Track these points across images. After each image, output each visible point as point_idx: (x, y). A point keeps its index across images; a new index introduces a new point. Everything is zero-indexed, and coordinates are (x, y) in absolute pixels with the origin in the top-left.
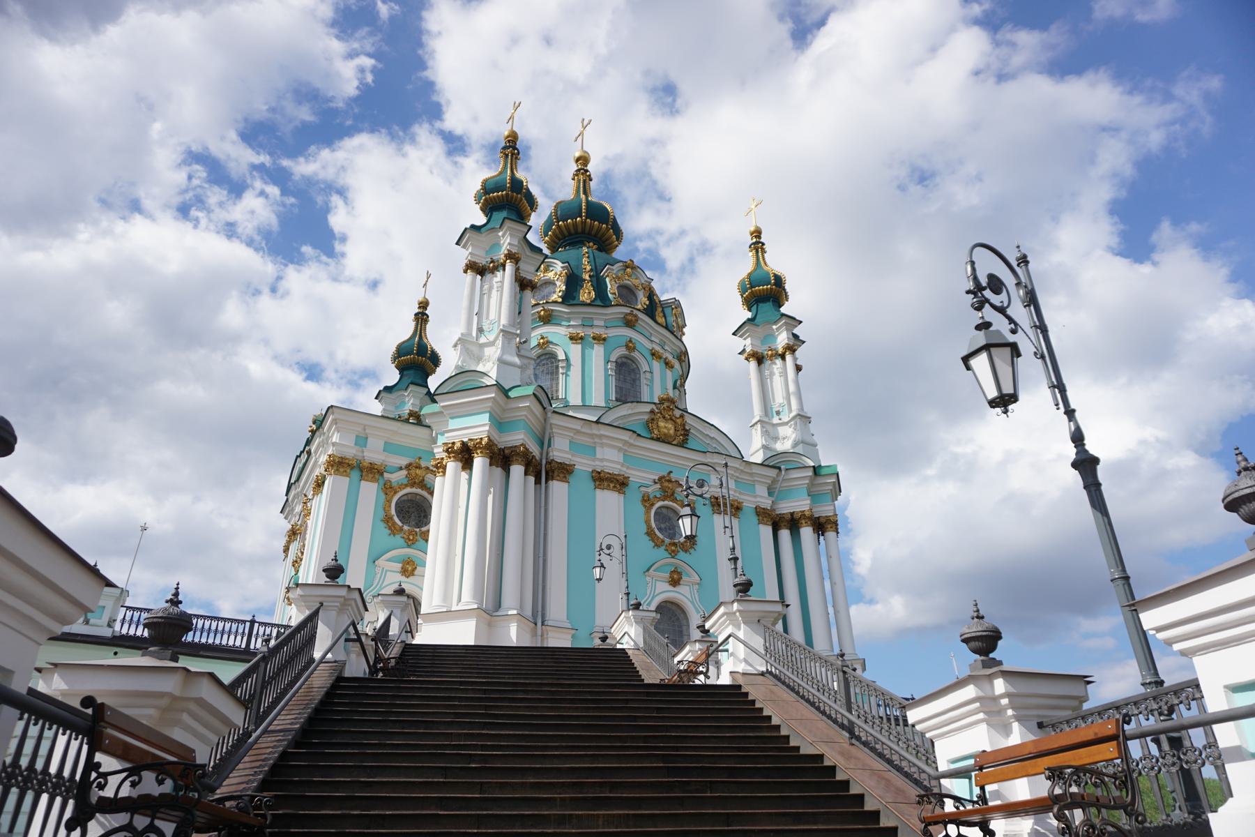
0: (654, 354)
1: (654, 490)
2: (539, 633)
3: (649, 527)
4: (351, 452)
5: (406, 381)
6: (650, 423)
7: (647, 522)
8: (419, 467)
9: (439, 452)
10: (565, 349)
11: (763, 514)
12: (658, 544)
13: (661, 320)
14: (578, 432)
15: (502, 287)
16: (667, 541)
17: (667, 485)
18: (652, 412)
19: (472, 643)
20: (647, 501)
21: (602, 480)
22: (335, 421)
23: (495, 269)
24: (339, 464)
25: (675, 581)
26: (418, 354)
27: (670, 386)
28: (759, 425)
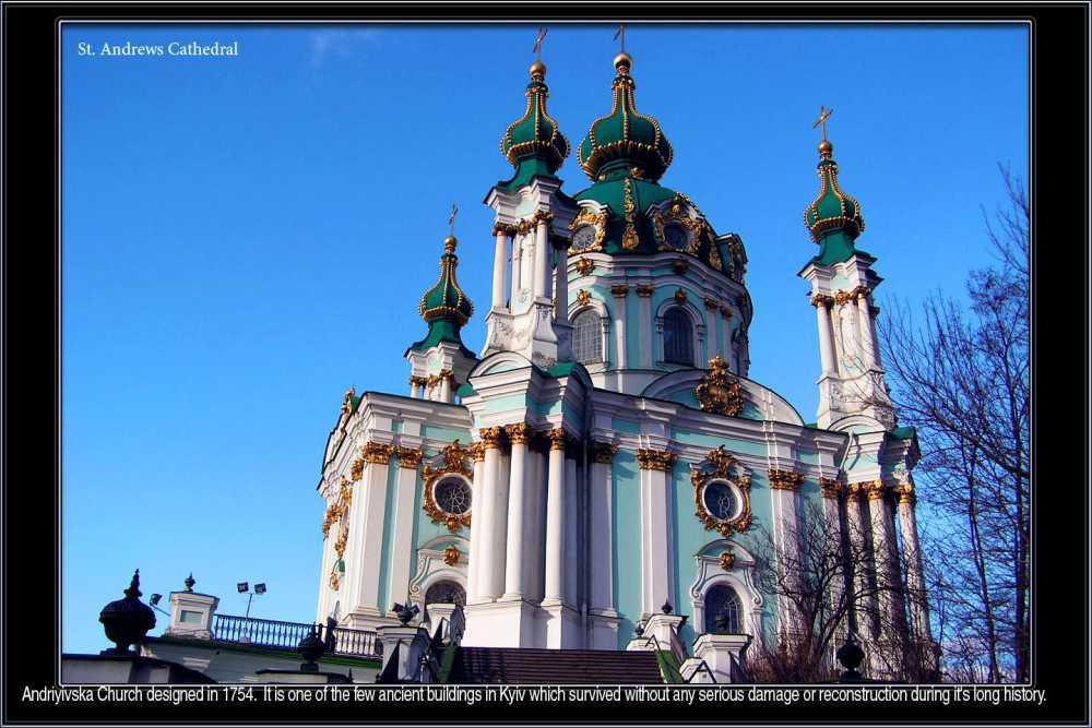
2: (585, 621)
3: (701, 507)
7: (698, 501)
8: (457, 450)
9: (476, 437)
11: (827, 485)
12: (711, 525)
13: (715, 261)
14: (619, 408)
15: (534, 251)
16: (720, 521)
19: (517, 646)
20: (700, 479)
21: (648, 458)
26: (447, 305)
27: (726, 338)
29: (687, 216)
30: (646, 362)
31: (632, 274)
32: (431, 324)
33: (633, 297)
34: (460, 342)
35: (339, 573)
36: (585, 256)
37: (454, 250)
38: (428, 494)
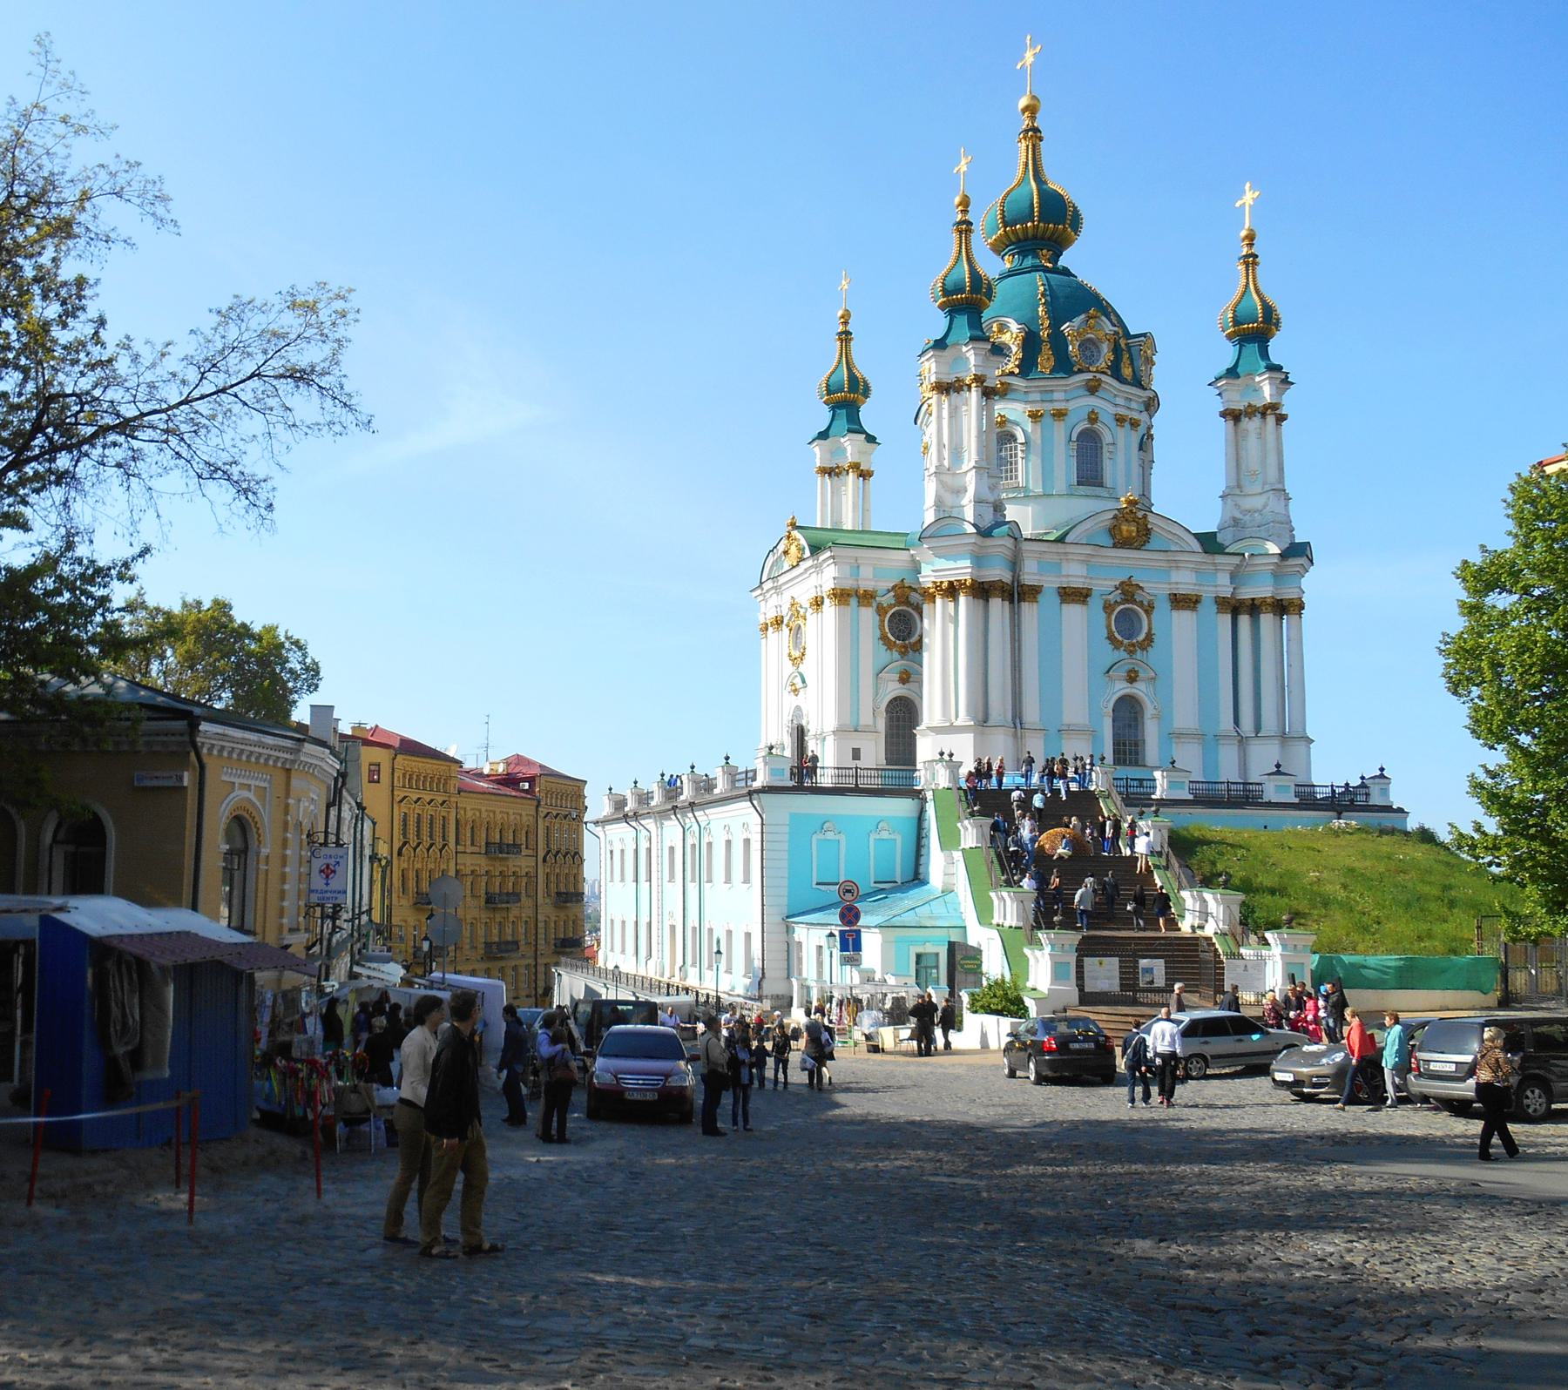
0: (1120, 420)
1: (1116, 596)
4: (848, 584)
5: (842, 423)
6: (1113, 531)
11: (1223, 604)
17: (1128, 590)
18: (1115, 517)
20: (1108, 608)
22: (833, 557)
23: (959, 390)
25: (1132, 678)
28: (1229, 500)
30: (1060, 486)
31: (1048, 397)
32: (833, 409)
33: (1048, 420)
34: (862, 431)
35: (799, 684)
36: (1004, 379)
38: (881, 627)
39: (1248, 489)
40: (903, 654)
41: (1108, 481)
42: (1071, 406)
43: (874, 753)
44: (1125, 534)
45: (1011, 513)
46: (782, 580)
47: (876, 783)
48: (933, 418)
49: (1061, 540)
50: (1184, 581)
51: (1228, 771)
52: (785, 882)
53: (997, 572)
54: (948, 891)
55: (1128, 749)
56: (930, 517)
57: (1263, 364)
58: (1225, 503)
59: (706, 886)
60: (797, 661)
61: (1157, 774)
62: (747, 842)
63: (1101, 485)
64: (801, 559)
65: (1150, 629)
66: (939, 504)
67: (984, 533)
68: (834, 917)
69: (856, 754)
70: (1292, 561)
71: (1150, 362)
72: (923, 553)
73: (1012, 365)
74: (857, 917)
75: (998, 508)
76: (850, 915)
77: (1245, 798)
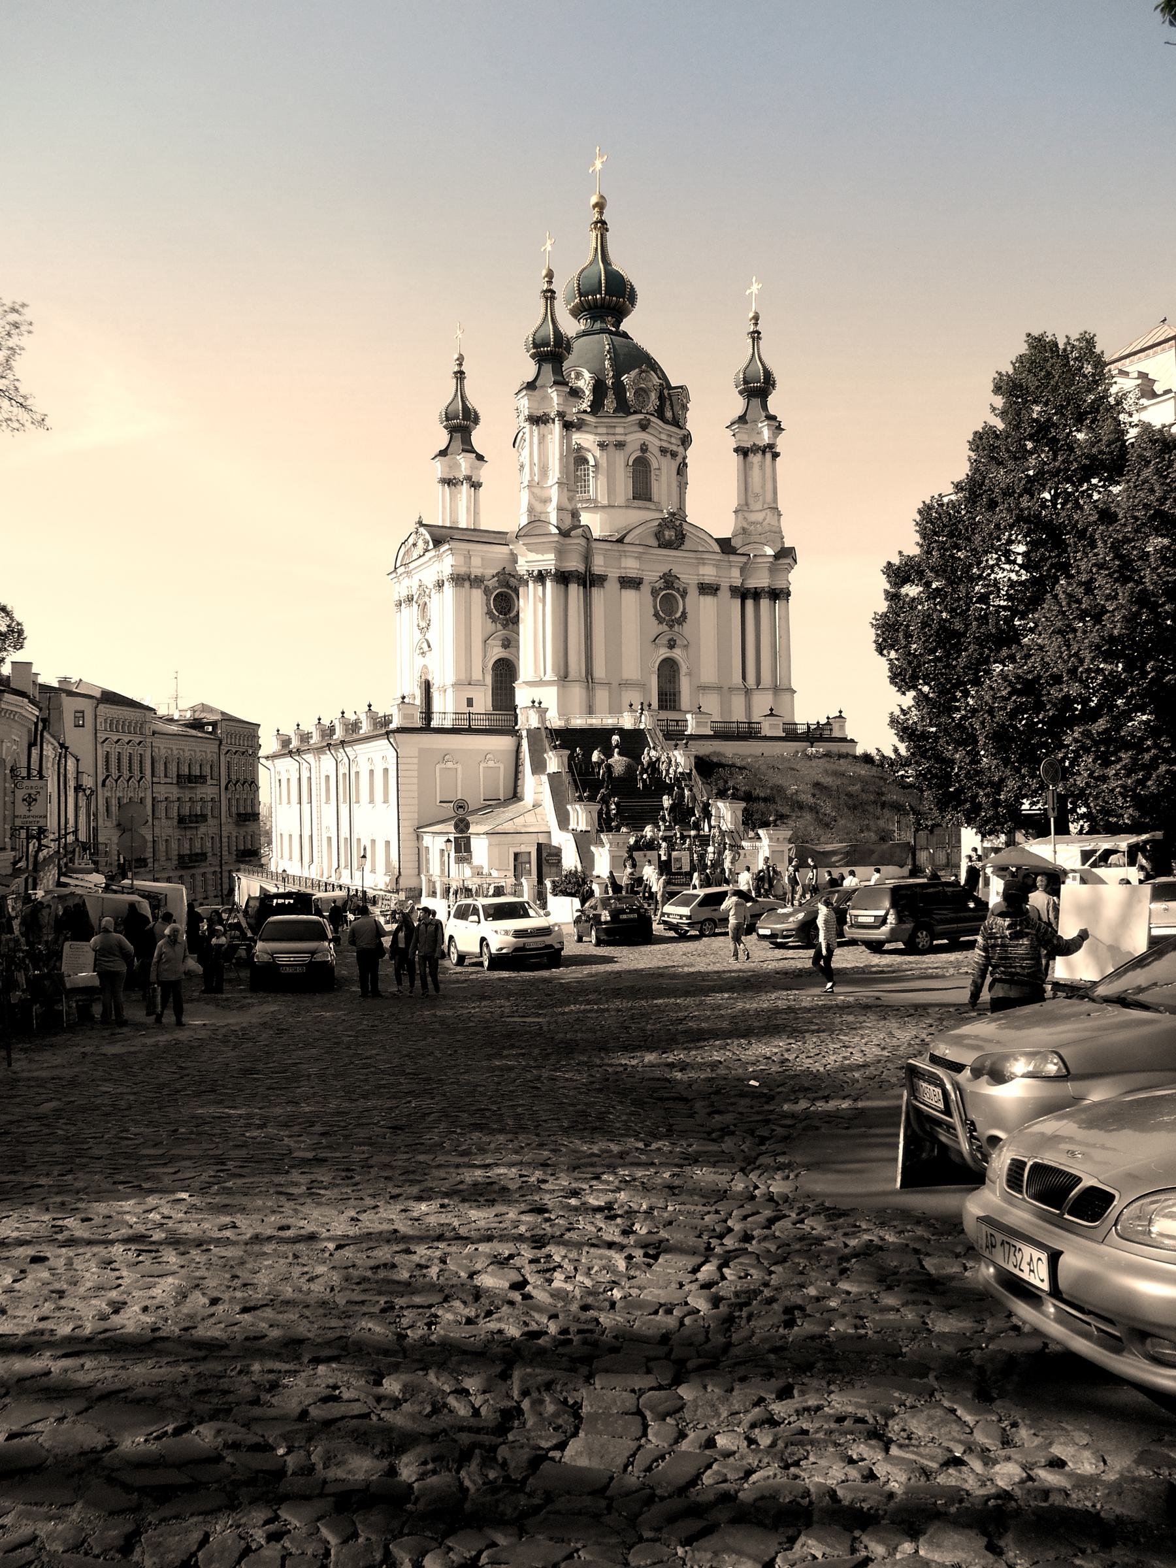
0: (663, 451)
4: (463, 570)
6: (658, 535)
7: (655, 607)
10: (594, 454)
12: (660, 620)
17: (669, 580)
20: (655, 592)
22: (451, 549)
23: (546, 422)
24: (458, 579)
25: (672, 645)
28: (740, 514)
29: (650, 381)
30: (620, 500)
31: (611, 431)
32: (451, 432)
33: (611, 448)
34: (474, 451)
35: (425, 646)
36: (580, 416)
37: (460, 365)
38: (488, 604)
39: (752, 507)
40: (505, 626)
41: (655, 498)
42: (629, 438)
43: (483, 701)
44: (667, 537)
45: (586, 518)
46: (412, 566)
47: (484, 724)
48: (527, 444)
49: (620, 541)
50: (708, 573)
51: (738, 714)
52: (416, 801)
53: (574, 564)
54: (536, 805)
55: (668, 699)
56: (524, 521)
57: (764, 414)
58: (737, 517)
59: (355, 806)
60: (424, 630)
61: (689, 717)
62: (386, 770)
63: (650, 500)
64: (427, 550)
65: (684, 609)
66: (531, 510)
67: (564, 534)
68: (450, 827)
69: (470, 702)
70: (782, 561)
71: (685, 408)
72: (519, 548)
73: (585, 405)
74: (467, 826)
75: (575, 515)
76: (462, 826)
77: (749, 733)
